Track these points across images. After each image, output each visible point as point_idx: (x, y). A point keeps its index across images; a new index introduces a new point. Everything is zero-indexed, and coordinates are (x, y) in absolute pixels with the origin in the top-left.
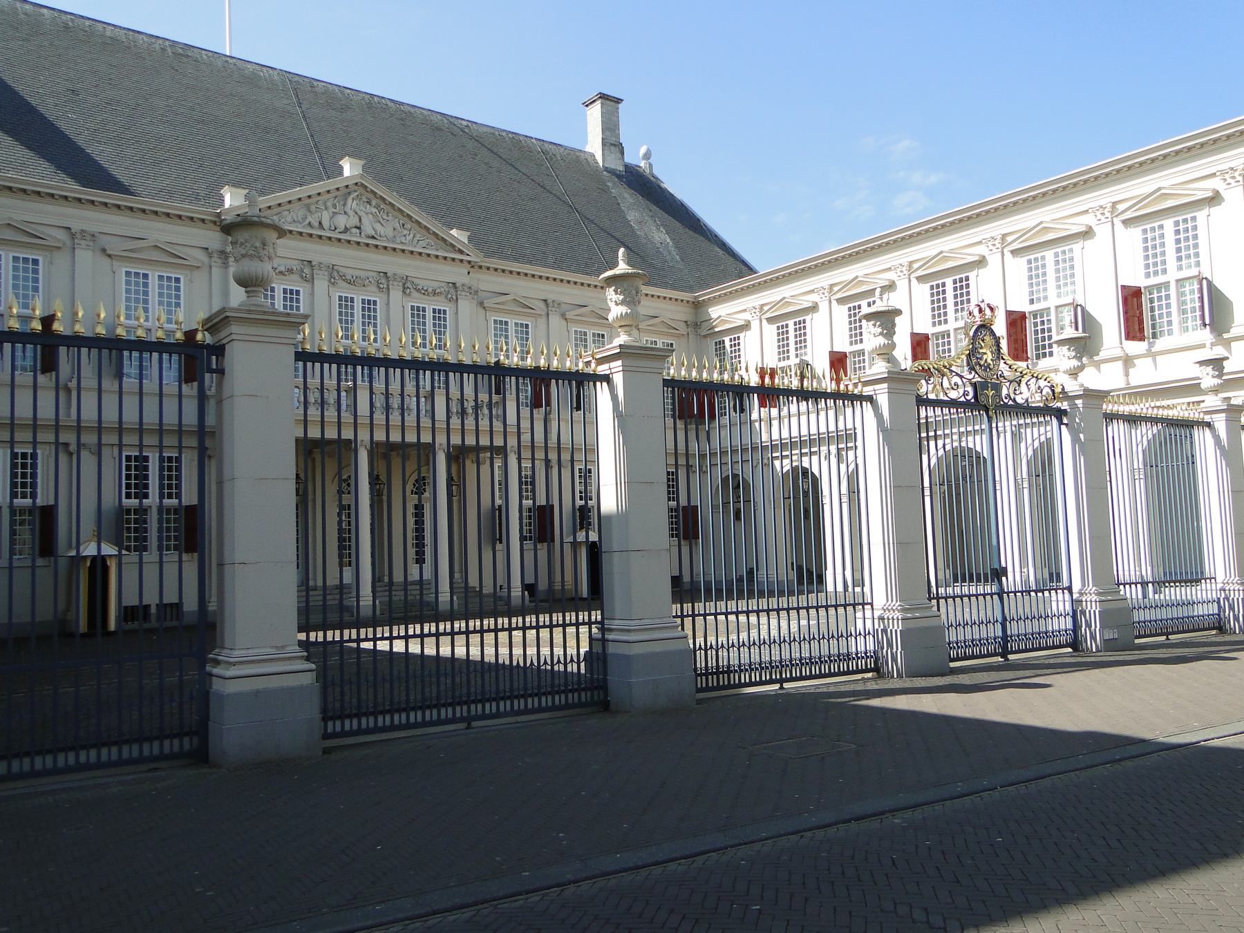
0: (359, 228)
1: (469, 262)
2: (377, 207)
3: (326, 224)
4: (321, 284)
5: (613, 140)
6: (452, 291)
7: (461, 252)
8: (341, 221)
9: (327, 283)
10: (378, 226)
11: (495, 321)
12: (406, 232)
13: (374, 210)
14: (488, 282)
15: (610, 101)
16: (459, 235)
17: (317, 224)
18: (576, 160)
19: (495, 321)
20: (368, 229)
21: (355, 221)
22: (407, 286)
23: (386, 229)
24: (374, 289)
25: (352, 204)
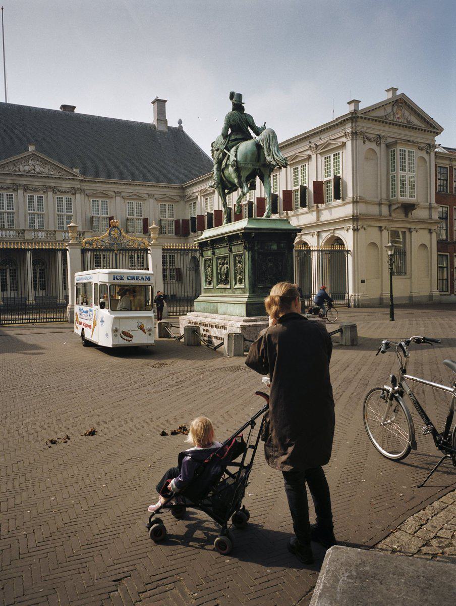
0: (34, 170)
3: (21, 170)
4: (21, 192)
7: (76, 176)
8: (27, 168)
9: (23, 191)
10: (42, 169)
17: (17, 170)
20: (38, 169)
22: (55, 190)
23: (46, 170)
24: (41, 192)
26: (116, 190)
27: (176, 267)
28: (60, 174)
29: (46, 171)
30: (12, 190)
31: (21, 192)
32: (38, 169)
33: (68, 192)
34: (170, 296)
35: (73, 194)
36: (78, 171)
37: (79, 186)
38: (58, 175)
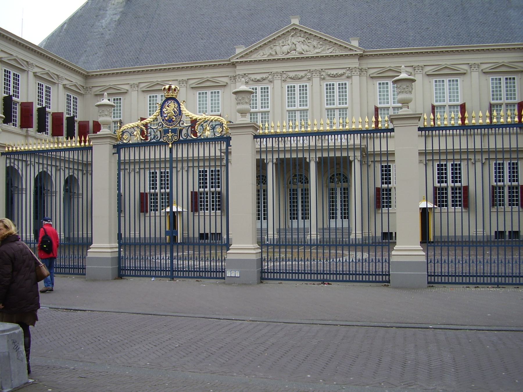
1: (357, 54)
4: (277, 82)
8: (286, 49)
10: (305, 47)
12: (320, 46)
13: (302, 39)
17: (274, 53)
20: (299, 49)
26: (415, 64)
27: (464, 183)
28: (330, 50)
29: (311, 48)
31: (277, 82)
32: (300, 48)
33: (341, 75)
34: (507, 234)
35: (348, 77)
36: (355, 43)
37: (357, 66)
38: (327, 53)
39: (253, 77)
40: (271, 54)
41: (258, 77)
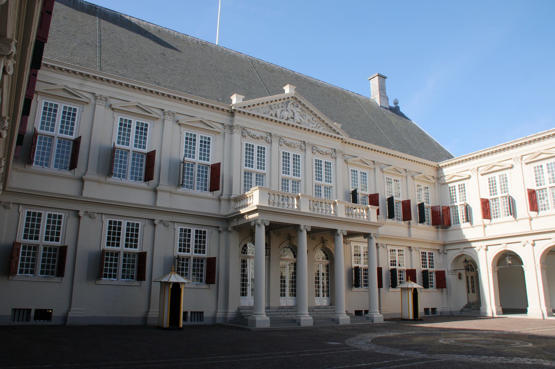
0: (293, 118)
1: (342, 139)
2: (301, 109)
3: (278, 115)
4: (275, 144)
5: (383, 94)
6: (334, 153)
7: (338, 133)
8: (286, 114)
10: (301, 118)
11: (352, 170)
12: (314, 122)
14: (350, 150)
15: (382, 77)
16: (337, 126)
17: (274, 115)
18: (368, 103)
19: (352, 170)
20: (297, 118)
21: (291, 115)
24: (298, 149)
25: (290, 107)
30: (265, 142)
39: (253, 132)
40: (271, 115)
41: (258, 134)
